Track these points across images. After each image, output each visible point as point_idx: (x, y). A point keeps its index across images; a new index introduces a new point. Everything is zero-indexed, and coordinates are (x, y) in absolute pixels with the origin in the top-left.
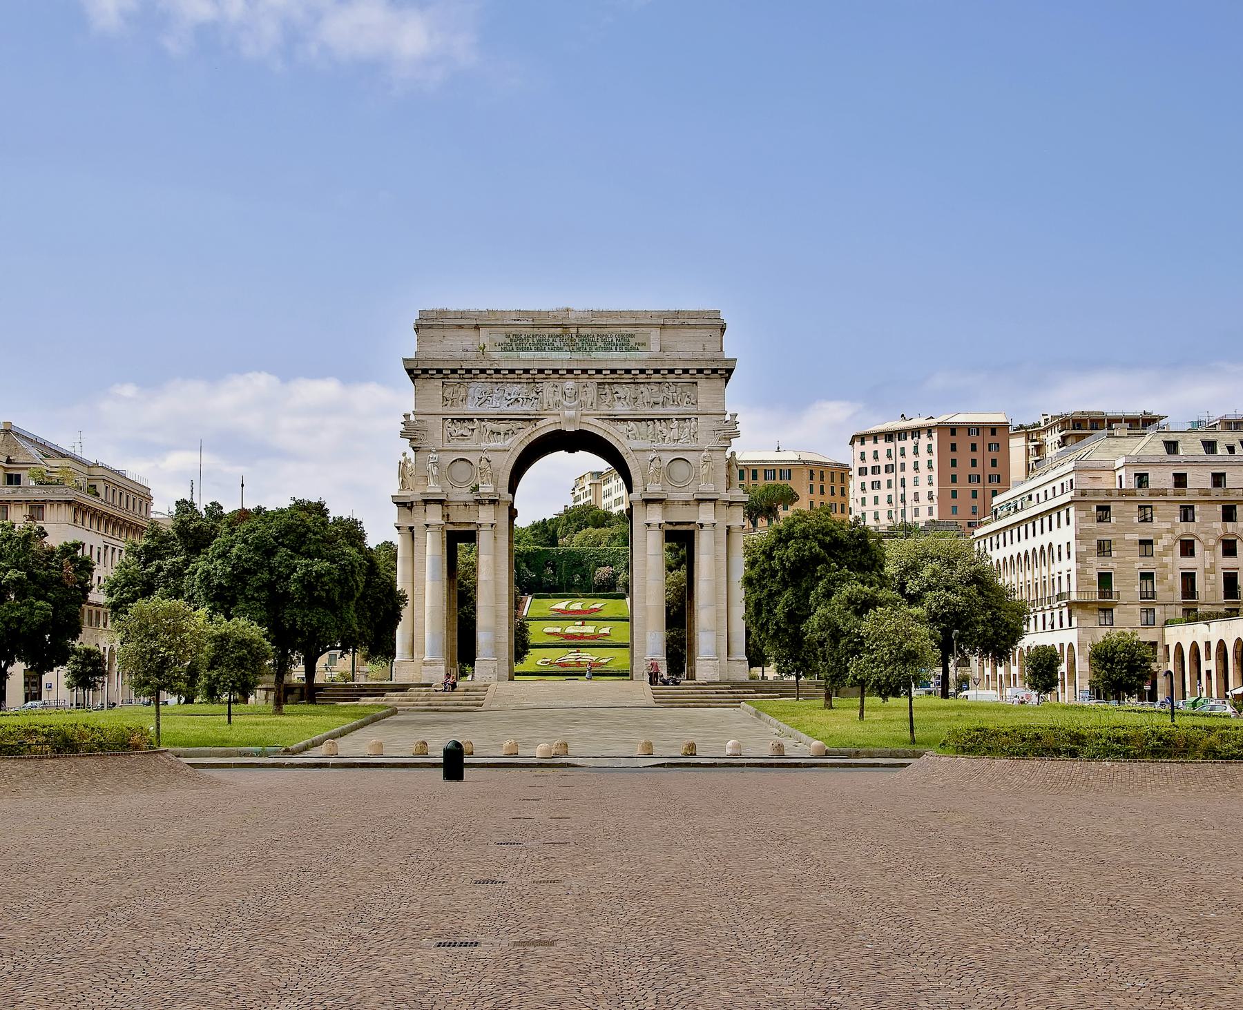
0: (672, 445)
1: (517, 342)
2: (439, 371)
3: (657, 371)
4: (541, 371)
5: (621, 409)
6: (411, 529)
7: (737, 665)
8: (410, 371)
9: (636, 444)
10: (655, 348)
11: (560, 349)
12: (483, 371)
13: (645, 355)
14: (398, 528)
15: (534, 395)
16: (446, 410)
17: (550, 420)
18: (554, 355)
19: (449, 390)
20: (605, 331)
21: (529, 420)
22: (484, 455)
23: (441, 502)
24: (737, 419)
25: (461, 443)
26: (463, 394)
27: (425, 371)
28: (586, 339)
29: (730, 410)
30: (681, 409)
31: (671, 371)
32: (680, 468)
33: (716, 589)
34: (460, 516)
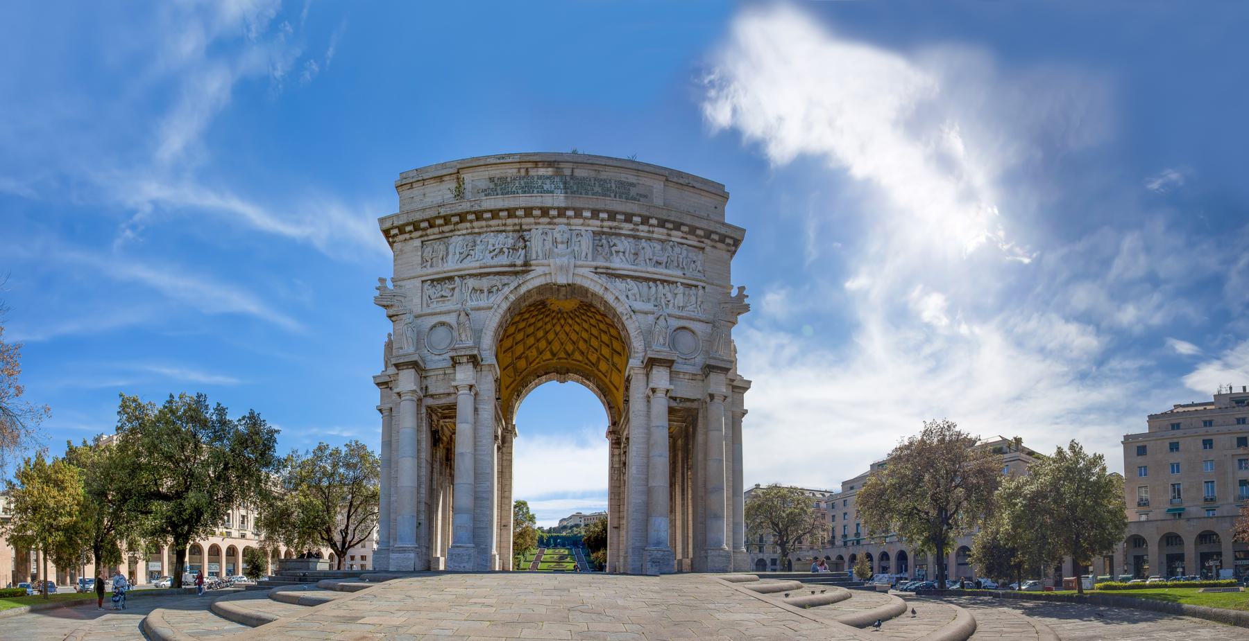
9: (638, 305)
20: (604, 175)
23: (415, 365)
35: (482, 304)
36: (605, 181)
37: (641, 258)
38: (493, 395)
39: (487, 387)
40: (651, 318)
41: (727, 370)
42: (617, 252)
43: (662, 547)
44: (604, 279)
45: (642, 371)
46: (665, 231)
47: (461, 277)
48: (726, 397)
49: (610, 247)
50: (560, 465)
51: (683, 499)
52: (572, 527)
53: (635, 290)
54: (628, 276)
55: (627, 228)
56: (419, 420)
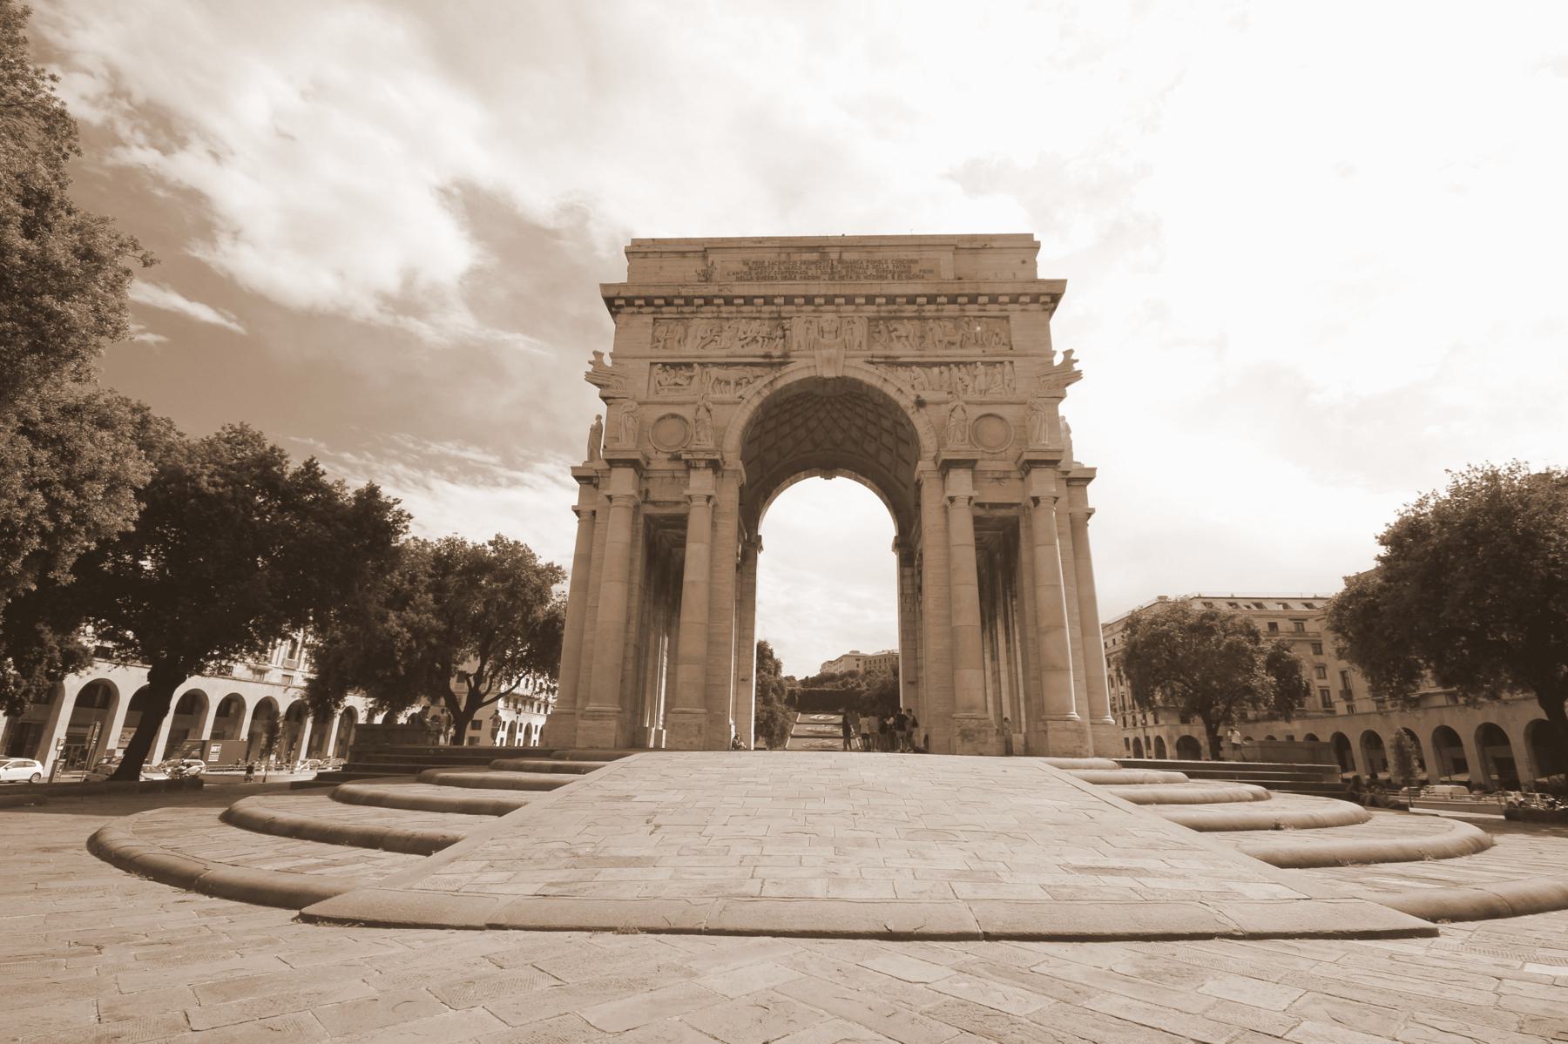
0: (977, 397)
2: (649, 301)
3: (953, 299)
4: (789, 300)
5: (901, 350)
6: (594, 513)
7: (1103, 732)
8: (609, 302)
9: (925, 396)
10: (947, 274)
11: (813, 278)
12: (708, 301)
14: (577, 512)
15: (780, 333)
16: (655, 352)
17: (801, 363)
19: (664, 328)
20: (878, 256)
23: (633, 464)
24: (1074, 357)
27: (630, 302)
28: (851, 266)
30: (989, 351)
31: (973, 299)
32: (992, 429)
35: (727, 397)
38: (735, 506)
39: (730, 497)
40: (945, 409)
41: (1055, 463)
42: (899, 337)
44: (882, 368)
45: (936, 474)
46: (957, 307)
47: (701, 364)
48: (1057, 498)
50: (825, 570)
51: (1008, 641)
52: (843, 676)
54: (913, 364)
55: (910, 310)
56: (634, 532)
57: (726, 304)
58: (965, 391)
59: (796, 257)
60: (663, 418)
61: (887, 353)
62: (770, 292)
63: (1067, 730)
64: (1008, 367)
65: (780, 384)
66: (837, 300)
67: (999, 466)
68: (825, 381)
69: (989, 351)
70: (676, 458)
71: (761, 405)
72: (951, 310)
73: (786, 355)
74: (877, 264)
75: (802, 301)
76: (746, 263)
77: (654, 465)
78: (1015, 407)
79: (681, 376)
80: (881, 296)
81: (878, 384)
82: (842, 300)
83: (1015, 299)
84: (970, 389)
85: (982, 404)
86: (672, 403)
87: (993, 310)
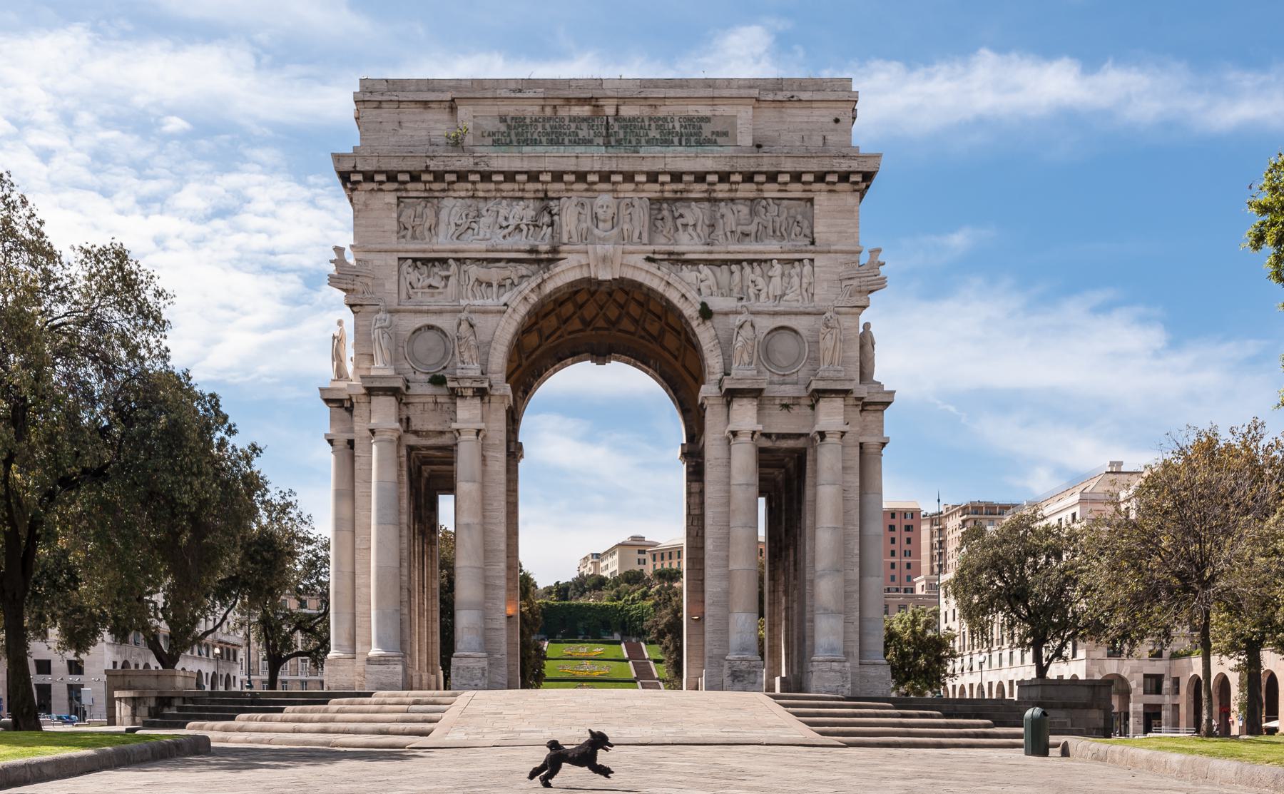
0: (770, 306)
1: (516, 132)
3: (749, 177)
4: (558, 176)
5: (689, 244)
9: (716, 303)
10: (746, 140)
11: (588, 142)
13: (729, 151)
15: (546, 219)
18: (579, 149)
20: (662, 111)
21: (539, 261)
22: (463, 316)
25: (428, 299)
26: (430, 220)
29: (867, 242)
31: (772, 177)
33: (843, 544)
34: (425, 420)
36: (665, 119)
37: (719, 232)
42: (685, 226)
43: (747, 656)
44: (665, 267)
46: (754, 186)
49: (675, 218)
53: (711, 281)
55: (698, 190)
57: (482, 181)
58: (757, 296)
59: (563, 112)
60: (419, 329)
61: (671, 248)
62: (534, 166)
63: (831, 670)
64: (807, 268)
65: (549, 288)
66: (615, 178)
67: (789, 391)
68: (600, 283)
69: (787, 245)
70: (437, 381)
71: (528, 313)
72: (747, 190)
73: (554, 250)
74: (660, 122)
75: (572, 178)
76: (503, 119)
77: (416, 389)
78: (812, 318)
79: (434, 276)
80: (664, 173)
81: (661, 289)
82: (619, 178)
83: (820, 177)
84: (763, 295)
85: (775, 314)
86: (428, 312)
87: (796, 190)
